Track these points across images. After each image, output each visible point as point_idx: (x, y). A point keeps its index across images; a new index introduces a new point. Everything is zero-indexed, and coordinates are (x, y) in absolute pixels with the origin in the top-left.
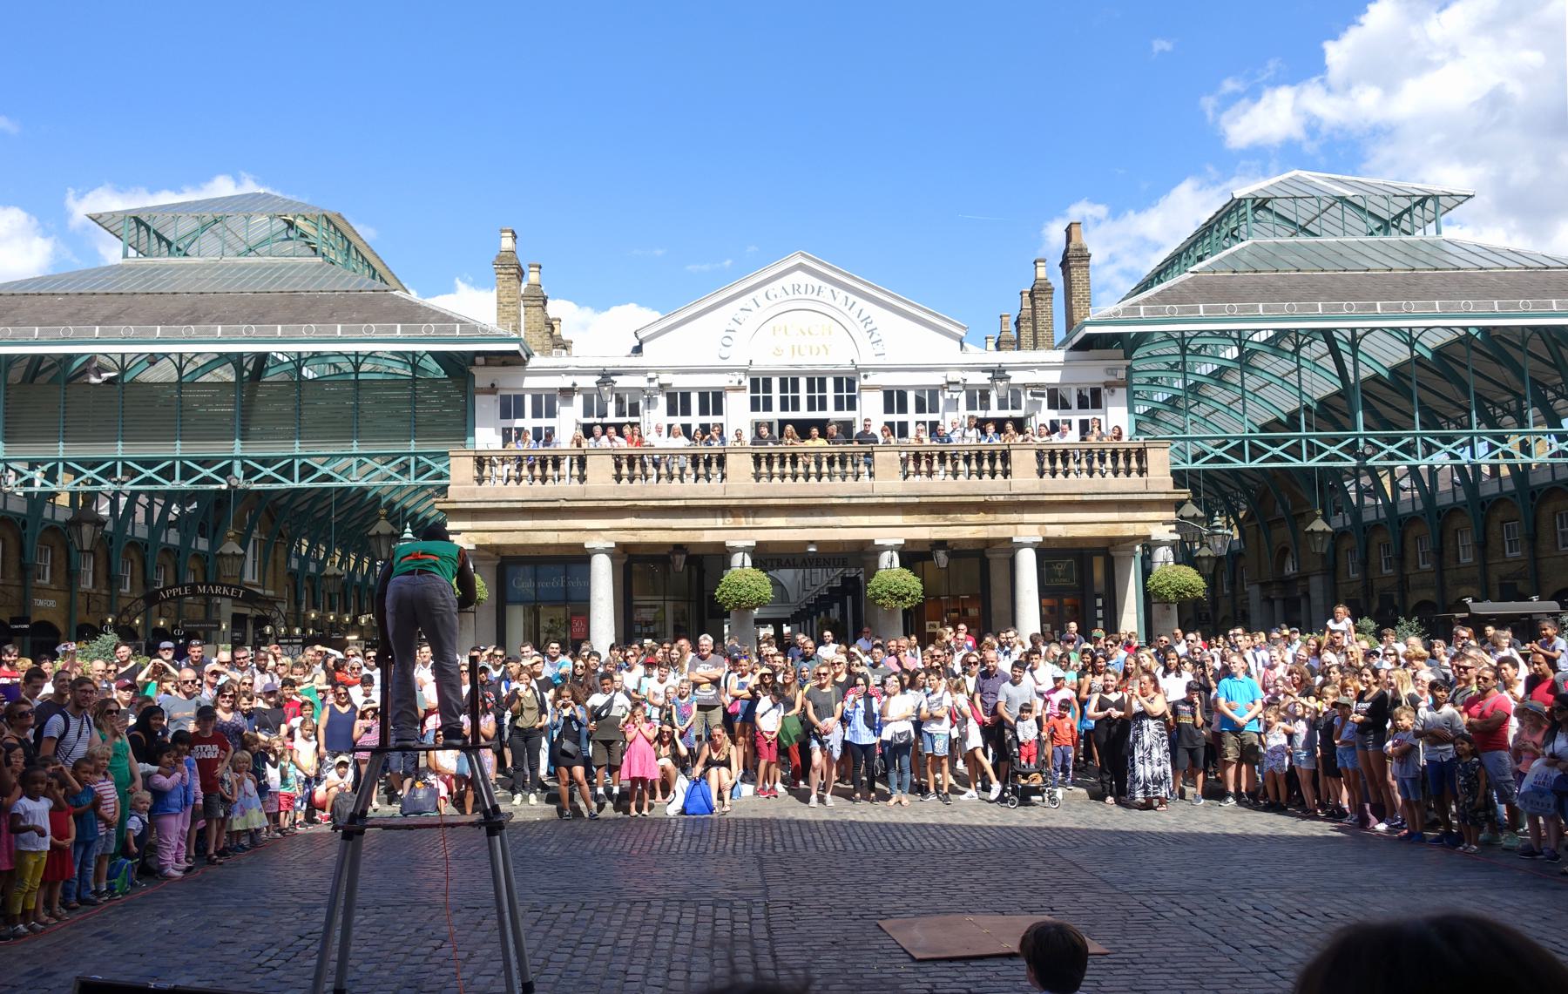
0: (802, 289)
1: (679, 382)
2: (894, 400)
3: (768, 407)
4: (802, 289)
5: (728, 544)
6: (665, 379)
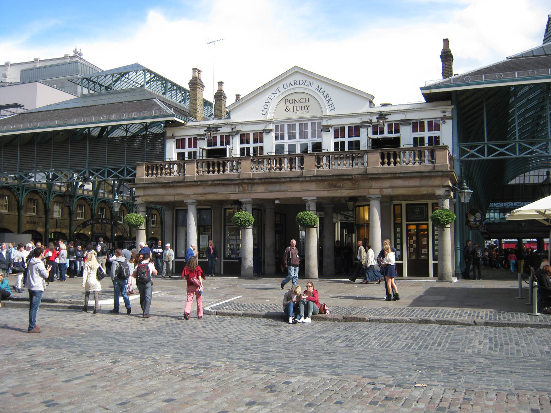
0: (298, 83)
1: (245, 129)
2: (339, 132)
3: (283, 138)
4: (298, 83)
5: (240, 200)
6: (238, 128)
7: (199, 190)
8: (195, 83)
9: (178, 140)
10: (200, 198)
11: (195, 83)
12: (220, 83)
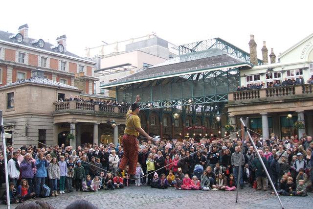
7: (269, 107)
8: (253, 44)
9: (248, 78)
10: (270, 111)
11: (253, 44)
12: (264, 42)
